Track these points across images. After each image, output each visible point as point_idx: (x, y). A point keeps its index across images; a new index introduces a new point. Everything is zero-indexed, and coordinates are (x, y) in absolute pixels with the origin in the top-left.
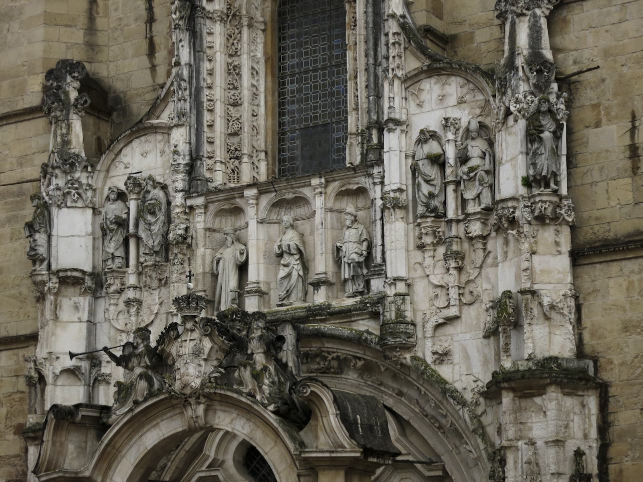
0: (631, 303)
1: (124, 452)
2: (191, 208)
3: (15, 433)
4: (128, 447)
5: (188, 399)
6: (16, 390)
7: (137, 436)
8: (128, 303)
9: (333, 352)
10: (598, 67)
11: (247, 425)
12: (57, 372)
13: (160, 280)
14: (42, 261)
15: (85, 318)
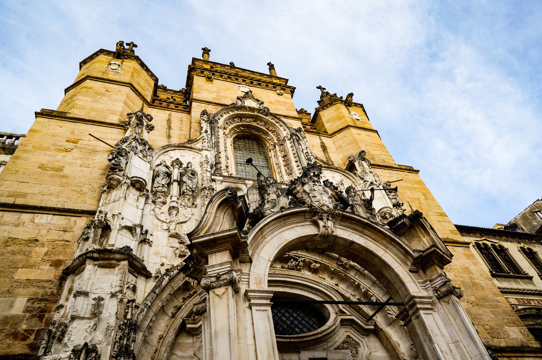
1: (267, 240)
2: (214, 180)
3: (51, 265)
4: (270, 237)
7: (277, 232)
8: (171, 208)
9: (302, 257)
12: (123, 225)
13: (193, 204)
15: (141, 206)
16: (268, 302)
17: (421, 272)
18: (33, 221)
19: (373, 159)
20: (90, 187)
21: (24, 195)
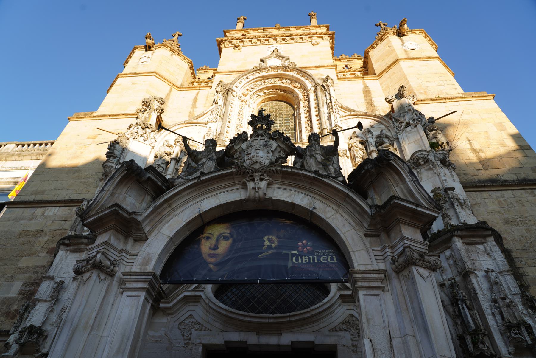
0: (505, 210)
5: (255, 174)
6: (61, 228)
10: (456, 112)
11: (307, 197)
14: (115, 158)
16: (146, 286)
17: (383, 235)
18: (43, 214)
19: (425, 93)
20: (96, 177)
21: (43, 192)
